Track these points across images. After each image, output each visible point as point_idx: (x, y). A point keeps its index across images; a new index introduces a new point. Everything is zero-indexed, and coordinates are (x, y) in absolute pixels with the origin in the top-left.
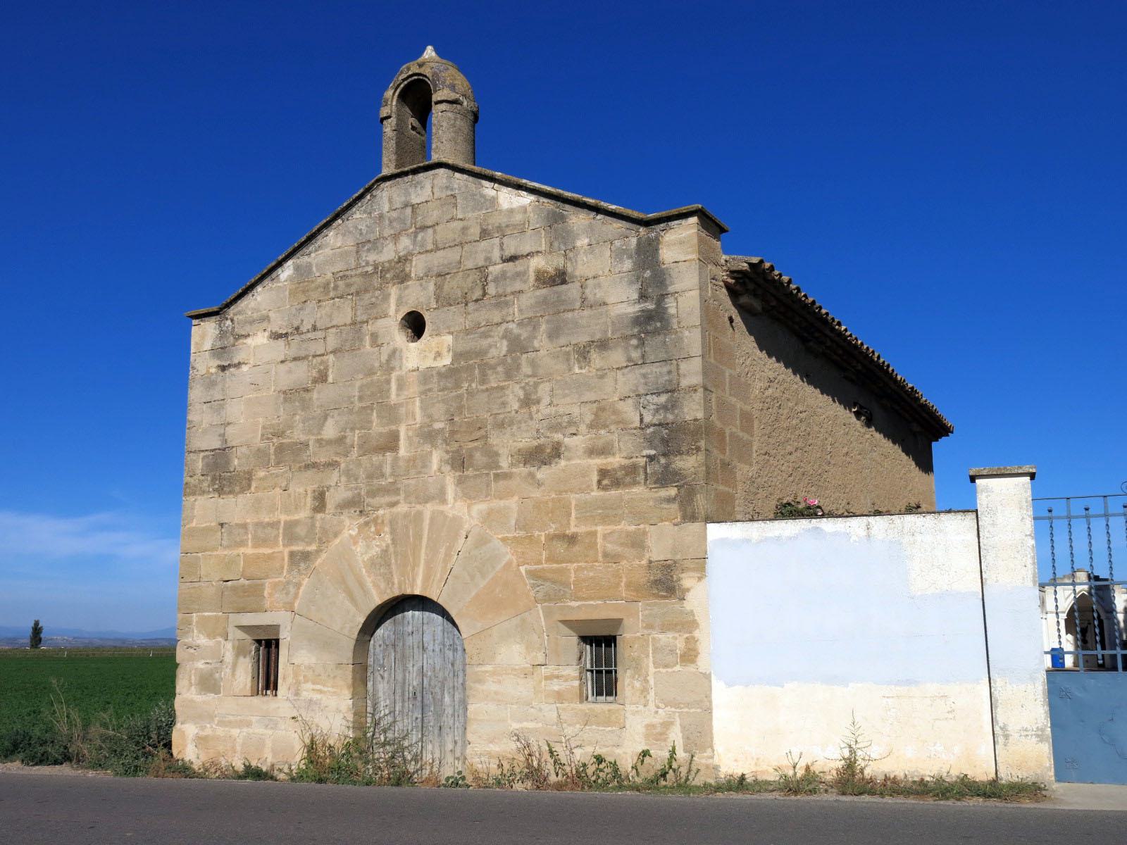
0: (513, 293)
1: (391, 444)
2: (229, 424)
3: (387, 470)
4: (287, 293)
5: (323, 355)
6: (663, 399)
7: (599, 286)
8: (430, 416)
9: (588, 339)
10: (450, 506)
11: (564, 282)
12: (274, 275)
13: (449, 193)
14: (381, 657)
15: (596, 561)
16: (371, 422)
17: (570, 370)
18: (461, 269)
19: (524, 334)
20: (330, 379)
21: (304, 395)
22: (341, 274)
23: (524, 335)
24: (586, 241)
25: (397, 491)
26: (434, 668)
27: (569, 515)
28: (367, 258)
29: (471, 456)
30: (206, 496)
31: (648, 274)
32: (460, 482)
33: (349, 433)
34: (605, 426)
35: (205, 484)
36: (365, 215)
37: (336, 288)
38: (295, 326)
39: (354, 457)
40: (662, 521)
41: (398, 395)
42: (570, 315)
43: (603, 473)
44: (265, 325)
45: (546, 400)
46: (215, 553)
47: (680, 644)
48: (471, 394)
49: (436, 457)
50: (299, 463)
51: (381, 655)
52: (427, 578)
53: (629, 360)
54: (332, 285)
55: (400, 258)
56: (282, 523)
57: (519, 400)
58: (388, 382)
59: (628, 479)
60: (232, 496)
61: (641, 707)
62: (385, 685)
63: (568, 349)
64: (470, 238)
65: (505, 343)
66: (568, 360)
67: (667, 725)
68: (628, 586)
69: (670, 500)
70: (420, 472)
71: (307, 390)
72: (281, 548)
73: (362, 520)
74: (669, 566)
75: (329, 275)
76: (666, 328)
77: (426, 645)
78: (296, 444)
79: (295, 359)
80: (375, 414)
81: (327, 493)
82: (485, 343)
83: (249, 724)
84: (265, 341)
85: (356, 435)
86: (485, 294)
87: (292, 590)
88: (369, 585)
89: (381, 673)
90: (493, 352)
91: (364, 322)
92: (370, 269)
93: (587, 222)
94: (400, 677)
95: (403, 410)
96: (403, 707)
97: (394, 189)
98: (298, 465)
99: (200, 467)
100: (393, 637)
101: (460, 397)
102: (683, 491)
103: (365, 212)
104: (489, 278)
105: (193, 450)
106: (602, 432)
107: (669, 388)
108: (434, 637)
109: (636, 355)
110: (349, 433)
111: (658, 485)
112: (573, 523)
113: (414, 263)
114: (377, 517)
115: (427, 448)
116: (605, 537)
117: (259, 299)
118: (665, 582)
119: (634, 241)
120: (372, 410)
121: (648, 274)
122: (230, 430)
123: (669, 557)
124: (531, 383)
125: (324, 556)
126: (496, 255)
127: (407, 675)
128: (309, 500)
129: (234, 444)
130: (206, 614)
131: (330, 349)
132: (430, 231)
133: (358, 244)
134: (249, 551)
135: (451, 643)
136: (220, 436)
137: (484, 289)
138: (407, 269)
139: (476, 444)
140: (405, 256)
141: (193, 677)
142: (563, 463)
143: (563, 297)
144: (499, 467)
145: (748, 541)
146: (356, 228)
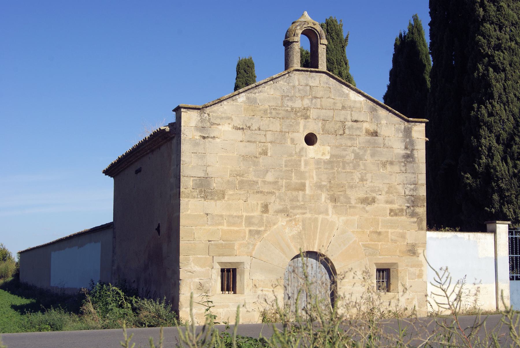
0: (356, 135)
1: (302, 187)
2: (209, 166)
3: (300, 199)
4: (243, 108)
5: (265, 143)
6: (413, 186)
7: (390, 140)
8: (320, 179)
9: (386, 160)
10: (330, 216)
11: (377, 136)
12: (234, 98)
16: (292, 177)
17: (379, 170)
20: (269, 154)
21: (255, 159)
22: (274, 107)
23: (361, 153)
24: (385, 122)
25: (305, 208)
29: (339, 198)
30: (196, 199)
31: (408, 140)
32: (334, 207)
33: (280, 180)
34: (392, 193)
35: (195, 194)
36: (286, 84)
37: (271, 113)
38: (248, 126)
41: (305, 168)
42: (379, 149)
43: (391, 210)
44: (229, 121)
45: (370, 180)
46: (203, 227)
47: (417, 272)
48: (338, 172)
49: (324, 196)
53: (401, 170)
55: (304, 108)
57: (359, 178)
58: (300, 161)
59: (400, 214)
64: (337, 108)
65: (353, 155)
67: (413, 299)
68: (400, 251)
69: (414, 222)
70: (316, 202)
72: (244, 228)
73: (288, 219)
75: (267, 106)
76: (414, 161)
78: (251, 181)
79: (248, 141)
82: (344, 153)
83: (228, 306)
84: (230, 129)
86: (344, 133)
87: (251, 247)
92: (289, 109)
93: (385, 114)
95: (307, 175)
97: (301, 76)
98: (252, 191)
101: (334, 173)
103: (285, 82)
106: (391, 195)
109: (403, 169)
110: (280, 180)
112: (380, 228)
113: (311, 112)
115: (319, 192)
116: (391, 233)
117: (225, 107)
118: (412, 251)
119: (403, 127)
120: (292, 172)
121: (408, 140)
122: (209, 169)
123: (414, 242)
125: (268, 233)
126: (349, 118)
128: (259, 208)
129: (212, 176)
131: (268, 140)
132: (319, 100)
134: (225, 227)
138: (308, 114)
142: (376, 205)
144: (350, 203)
145: (438, 238)
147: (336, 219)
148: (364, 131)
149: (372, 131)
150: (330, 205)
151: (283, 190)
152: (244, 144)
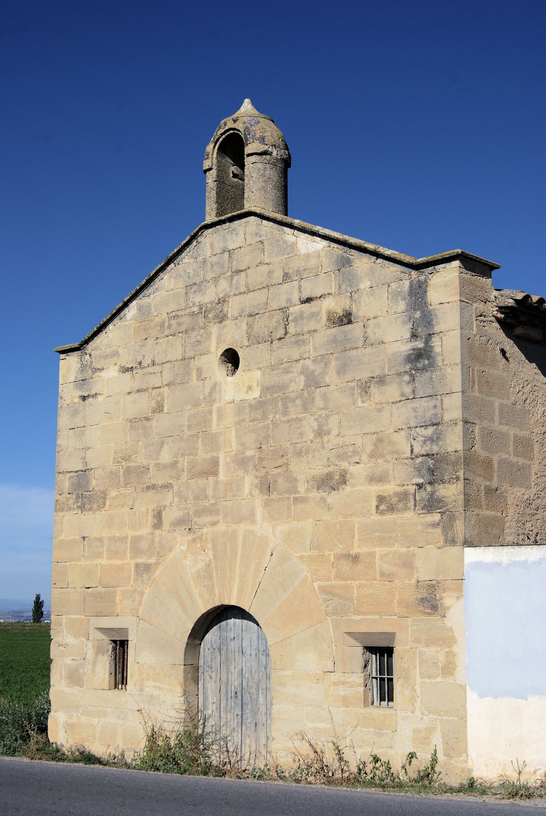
3: (210, 492)
5: (160, 387)
6: (430, 431)
7: (378, 326)
8: (243, 445)
10: (259, 526)
11: (350, 322)
12: (122, 314)
13: (258, 239)
14: (209, 659)
15: (375, 579)
16: (197, 449)
17: (354, 403)
18: (267, 310)
19: (318, 369)
20: (165, 410)
21: (146, 423)
22: (174, 314)
23: (318, 371)
24: (368, 284)
25: (217, 512)
26: (251, 671)
27: (353, 537)
28: (194, 300)
29: (275, 481)
30: (71, 512)
31: (418, 314)
32: (267, 504)
34: (382, 456)
35: (71, 502)
37: (170, 326)
38: (139, 361)
39: (184, 480)
40: (428, 544)
41: (218, 425)
42: (354, 353)
43: (381, 499)
44: (115, 359)
45: (335, 432)
46: (79, 563)
47: (442, 658)
49: (249, 482)
50: (142, 484)
51: (210, 658)
52: (241, 591)
53: (403, 395)
54: (167, 324)
55: (219, 299)
56: (129, 537)
57: (314, 431)
58: (210, 412)
59: (401, 505)
60: (91, 513)
61: (409, 713)
62: (213, 684)
63: (353, 384)
64: (275, 281)
65: (302, 378)
66: (353, 394)
67: (430, 730)
68: (400, 603)
69: (435, 525)
71: (147, 419)
72: (129, 560)
73: (190, 537)
74: (433, 586)
77: (244, 650)
78: (139, 467)
79: (138, 391)
80: (200, 442)
81: (163, 512)
82: (286, 378)
85: (186, 460)
87: (137, 598)
88: (196, 595)
89: (210, 673)
90: (293, 387)
91: (191, 358)
92: (196, 309)
93: (368, 266)
94: (224, 678)
95: (222, 439)
96: (227, 704)
97: (215, 235)
98: (141, 486)
99: (67, 487)
100: (218, 641)
101: (266, 427)
102: (445, 517)
104: (290, 319)
105: (61, 471)
106: (380, 461)
107: (435, 422)
108: (251, 642)
110: (180, 459)
111: (424, 511)
112: (356, 544)
113: (230, 304)
114: (202, 534)
115: (241, 473)
118: (430, 601)
119: (407, 283)
120: (198, 438)
121: (418, 314)
122: (89, 454)
124: (323, 415)
125: (161, 568)
127: (230, 676)
130: (73, 616)
131: (165, 382)
132: (243, 274)
133: (186, 286)
134: (104, 561)
135: (265, 649)
136: (82, 458)
137: (286, 328)
138: (225, 310)
139: (279, 470)
140: (224, 298)
141: (63, 672)
143: (349, 337)
144: (297, 492)
145: (498, 564)
146: (185, 271)
147: (268, 529)
148: (324, 318)
149: (341, 314)
150: (259, 502)
151: (185, 476)
152: (134, 396)
